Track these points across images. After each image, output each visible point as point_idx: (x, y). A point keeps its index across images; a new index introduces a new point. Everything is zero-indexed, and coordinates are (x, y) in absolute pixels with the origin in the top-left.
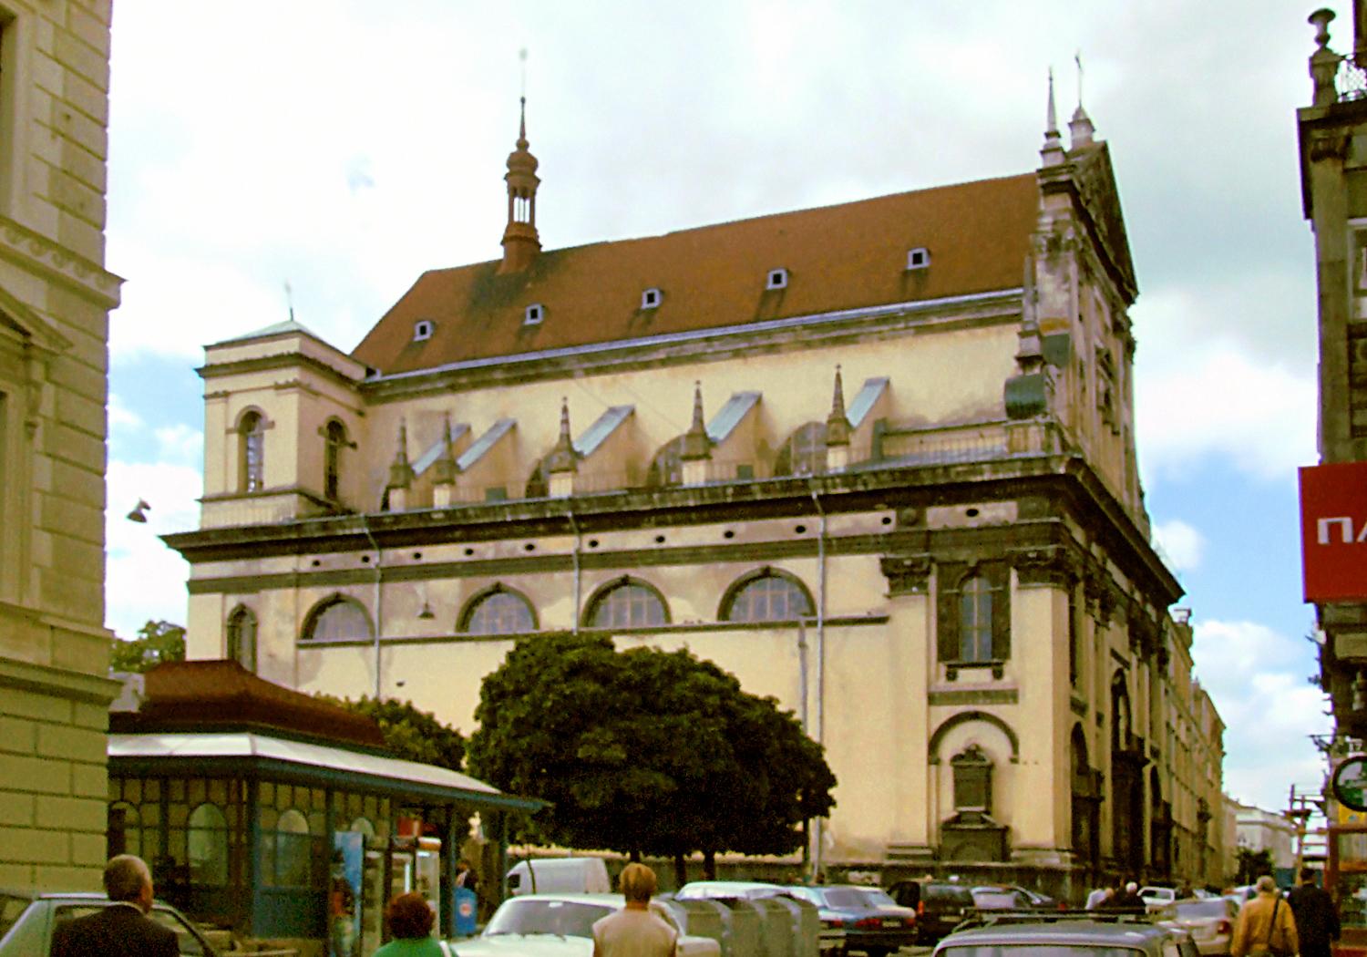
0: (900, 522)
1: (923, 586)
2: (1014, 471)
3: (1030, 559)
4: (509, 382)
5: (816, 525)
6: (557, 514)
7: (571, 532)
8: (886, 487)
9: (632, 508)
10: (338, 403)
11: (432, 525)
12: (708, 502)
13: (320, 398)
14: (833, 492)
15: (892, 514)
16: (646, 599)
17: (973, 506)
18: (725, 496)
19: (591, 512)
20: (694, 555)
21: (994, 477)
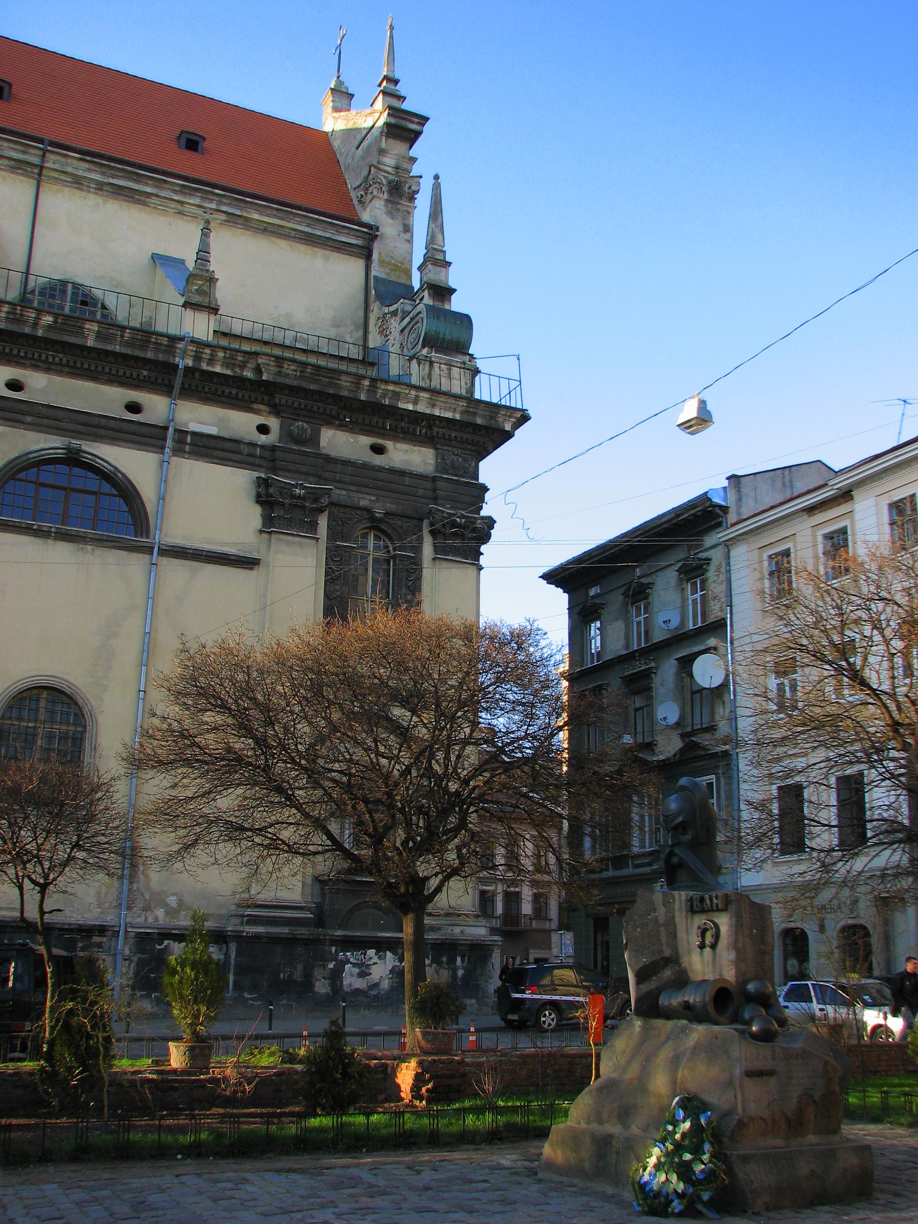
0: (287, 434)
1: (313, 527)
3: (454, 524)
5: (156, 407)
8: (287, 381)
14: (204, 366)
15: (273, 423)
17: (380, 441)
18: (35, 325)
21: (428, 411)
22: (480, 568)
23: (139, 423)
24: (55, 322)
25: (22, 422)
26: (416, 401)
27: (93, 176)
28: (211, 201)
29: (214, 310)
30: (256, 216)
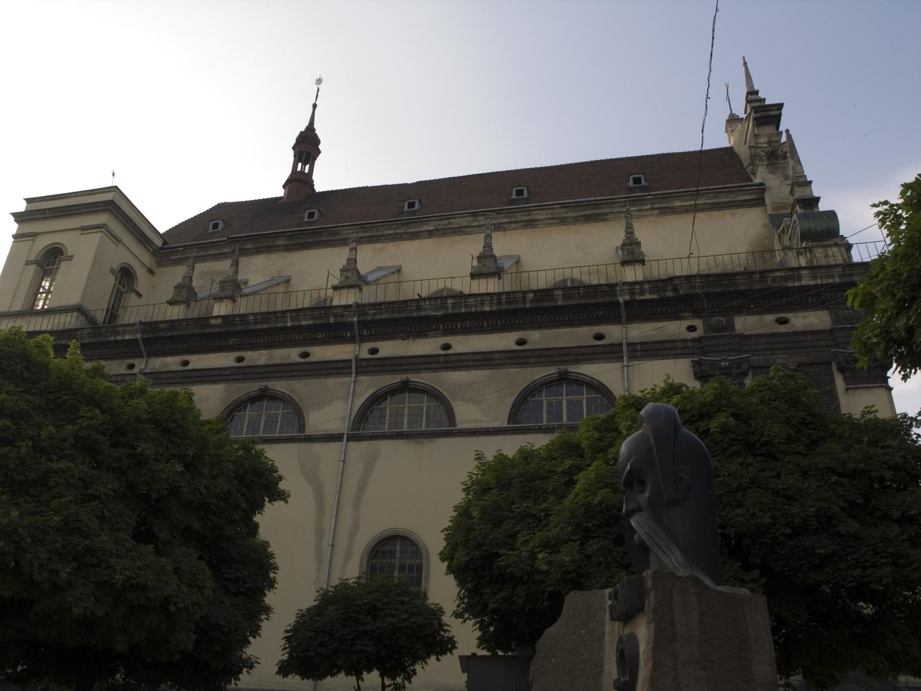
0: (708, 327)
2: (833, 276)
4: (289, 248)
5: (614, 332)
6: (340, 320)
7: (352, 340)
9: (423, 313)
10: (135, 255)
11: (208, 331)
12: (504, 307)
13: (121, 246)
14: (638, 297)
15: (698, 323)
16: (425, 403)
18: (524, 301)
19: (377, 317)
20: (484, 360)
21: (811, 283)
22: (890, 389)
23: (602, 345)
24: (535, 296)
25: (528, 363)
26: (799, 278)
27: (570, 214)
28: (646, 204)
29: (642, 262)
30: (678, 204)
